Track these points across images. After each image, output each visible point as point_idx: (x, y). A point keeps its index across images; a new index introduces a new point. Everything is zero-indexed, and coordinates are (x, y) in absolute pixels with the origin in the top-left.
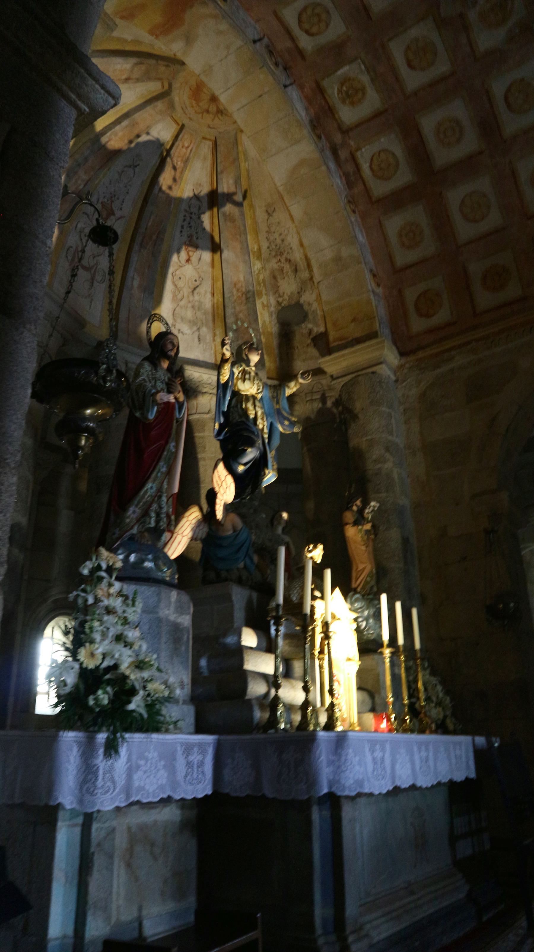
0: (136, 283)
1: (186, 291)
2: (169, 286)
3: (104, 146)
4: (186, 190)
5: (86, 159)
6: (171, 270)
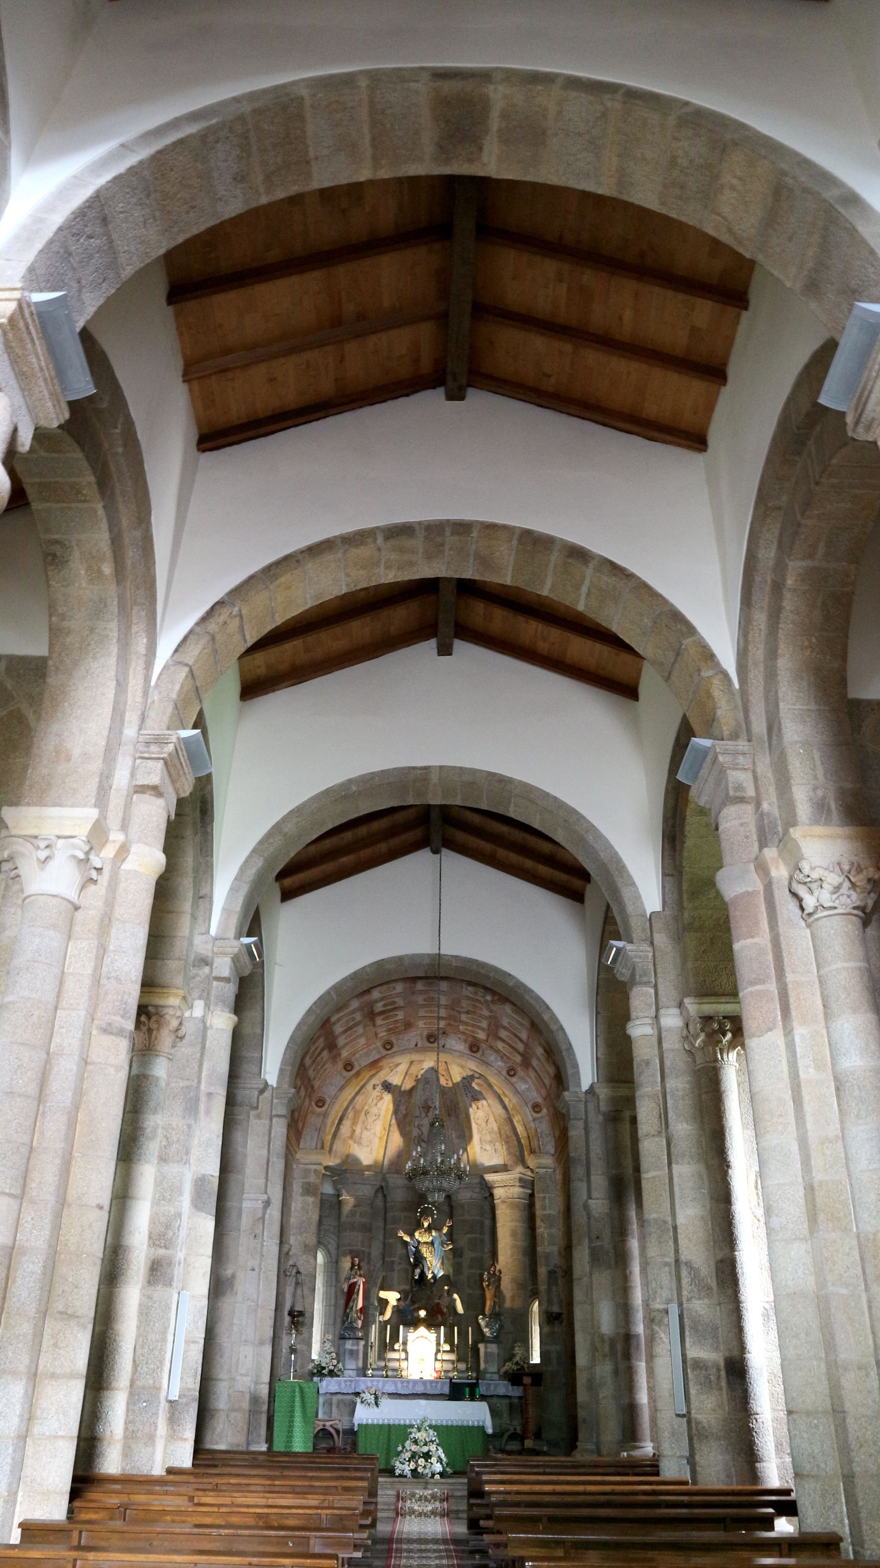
0: (454, 1136)
1: (484, 1124)
2: (474, 1126)
3: (405, 1091)
4: (457, 1078)
5: (400, 1101)
6: (472, 1117)
